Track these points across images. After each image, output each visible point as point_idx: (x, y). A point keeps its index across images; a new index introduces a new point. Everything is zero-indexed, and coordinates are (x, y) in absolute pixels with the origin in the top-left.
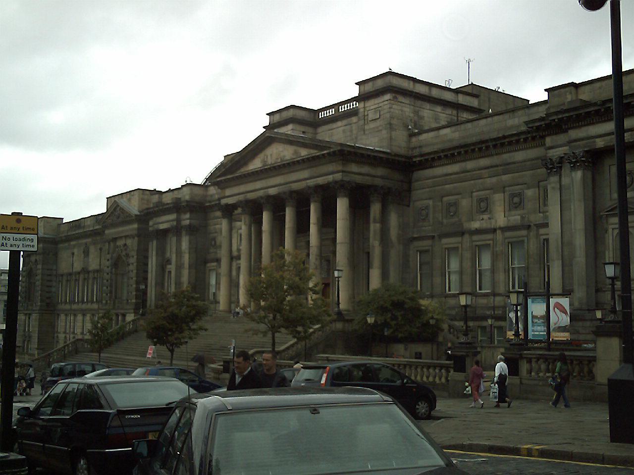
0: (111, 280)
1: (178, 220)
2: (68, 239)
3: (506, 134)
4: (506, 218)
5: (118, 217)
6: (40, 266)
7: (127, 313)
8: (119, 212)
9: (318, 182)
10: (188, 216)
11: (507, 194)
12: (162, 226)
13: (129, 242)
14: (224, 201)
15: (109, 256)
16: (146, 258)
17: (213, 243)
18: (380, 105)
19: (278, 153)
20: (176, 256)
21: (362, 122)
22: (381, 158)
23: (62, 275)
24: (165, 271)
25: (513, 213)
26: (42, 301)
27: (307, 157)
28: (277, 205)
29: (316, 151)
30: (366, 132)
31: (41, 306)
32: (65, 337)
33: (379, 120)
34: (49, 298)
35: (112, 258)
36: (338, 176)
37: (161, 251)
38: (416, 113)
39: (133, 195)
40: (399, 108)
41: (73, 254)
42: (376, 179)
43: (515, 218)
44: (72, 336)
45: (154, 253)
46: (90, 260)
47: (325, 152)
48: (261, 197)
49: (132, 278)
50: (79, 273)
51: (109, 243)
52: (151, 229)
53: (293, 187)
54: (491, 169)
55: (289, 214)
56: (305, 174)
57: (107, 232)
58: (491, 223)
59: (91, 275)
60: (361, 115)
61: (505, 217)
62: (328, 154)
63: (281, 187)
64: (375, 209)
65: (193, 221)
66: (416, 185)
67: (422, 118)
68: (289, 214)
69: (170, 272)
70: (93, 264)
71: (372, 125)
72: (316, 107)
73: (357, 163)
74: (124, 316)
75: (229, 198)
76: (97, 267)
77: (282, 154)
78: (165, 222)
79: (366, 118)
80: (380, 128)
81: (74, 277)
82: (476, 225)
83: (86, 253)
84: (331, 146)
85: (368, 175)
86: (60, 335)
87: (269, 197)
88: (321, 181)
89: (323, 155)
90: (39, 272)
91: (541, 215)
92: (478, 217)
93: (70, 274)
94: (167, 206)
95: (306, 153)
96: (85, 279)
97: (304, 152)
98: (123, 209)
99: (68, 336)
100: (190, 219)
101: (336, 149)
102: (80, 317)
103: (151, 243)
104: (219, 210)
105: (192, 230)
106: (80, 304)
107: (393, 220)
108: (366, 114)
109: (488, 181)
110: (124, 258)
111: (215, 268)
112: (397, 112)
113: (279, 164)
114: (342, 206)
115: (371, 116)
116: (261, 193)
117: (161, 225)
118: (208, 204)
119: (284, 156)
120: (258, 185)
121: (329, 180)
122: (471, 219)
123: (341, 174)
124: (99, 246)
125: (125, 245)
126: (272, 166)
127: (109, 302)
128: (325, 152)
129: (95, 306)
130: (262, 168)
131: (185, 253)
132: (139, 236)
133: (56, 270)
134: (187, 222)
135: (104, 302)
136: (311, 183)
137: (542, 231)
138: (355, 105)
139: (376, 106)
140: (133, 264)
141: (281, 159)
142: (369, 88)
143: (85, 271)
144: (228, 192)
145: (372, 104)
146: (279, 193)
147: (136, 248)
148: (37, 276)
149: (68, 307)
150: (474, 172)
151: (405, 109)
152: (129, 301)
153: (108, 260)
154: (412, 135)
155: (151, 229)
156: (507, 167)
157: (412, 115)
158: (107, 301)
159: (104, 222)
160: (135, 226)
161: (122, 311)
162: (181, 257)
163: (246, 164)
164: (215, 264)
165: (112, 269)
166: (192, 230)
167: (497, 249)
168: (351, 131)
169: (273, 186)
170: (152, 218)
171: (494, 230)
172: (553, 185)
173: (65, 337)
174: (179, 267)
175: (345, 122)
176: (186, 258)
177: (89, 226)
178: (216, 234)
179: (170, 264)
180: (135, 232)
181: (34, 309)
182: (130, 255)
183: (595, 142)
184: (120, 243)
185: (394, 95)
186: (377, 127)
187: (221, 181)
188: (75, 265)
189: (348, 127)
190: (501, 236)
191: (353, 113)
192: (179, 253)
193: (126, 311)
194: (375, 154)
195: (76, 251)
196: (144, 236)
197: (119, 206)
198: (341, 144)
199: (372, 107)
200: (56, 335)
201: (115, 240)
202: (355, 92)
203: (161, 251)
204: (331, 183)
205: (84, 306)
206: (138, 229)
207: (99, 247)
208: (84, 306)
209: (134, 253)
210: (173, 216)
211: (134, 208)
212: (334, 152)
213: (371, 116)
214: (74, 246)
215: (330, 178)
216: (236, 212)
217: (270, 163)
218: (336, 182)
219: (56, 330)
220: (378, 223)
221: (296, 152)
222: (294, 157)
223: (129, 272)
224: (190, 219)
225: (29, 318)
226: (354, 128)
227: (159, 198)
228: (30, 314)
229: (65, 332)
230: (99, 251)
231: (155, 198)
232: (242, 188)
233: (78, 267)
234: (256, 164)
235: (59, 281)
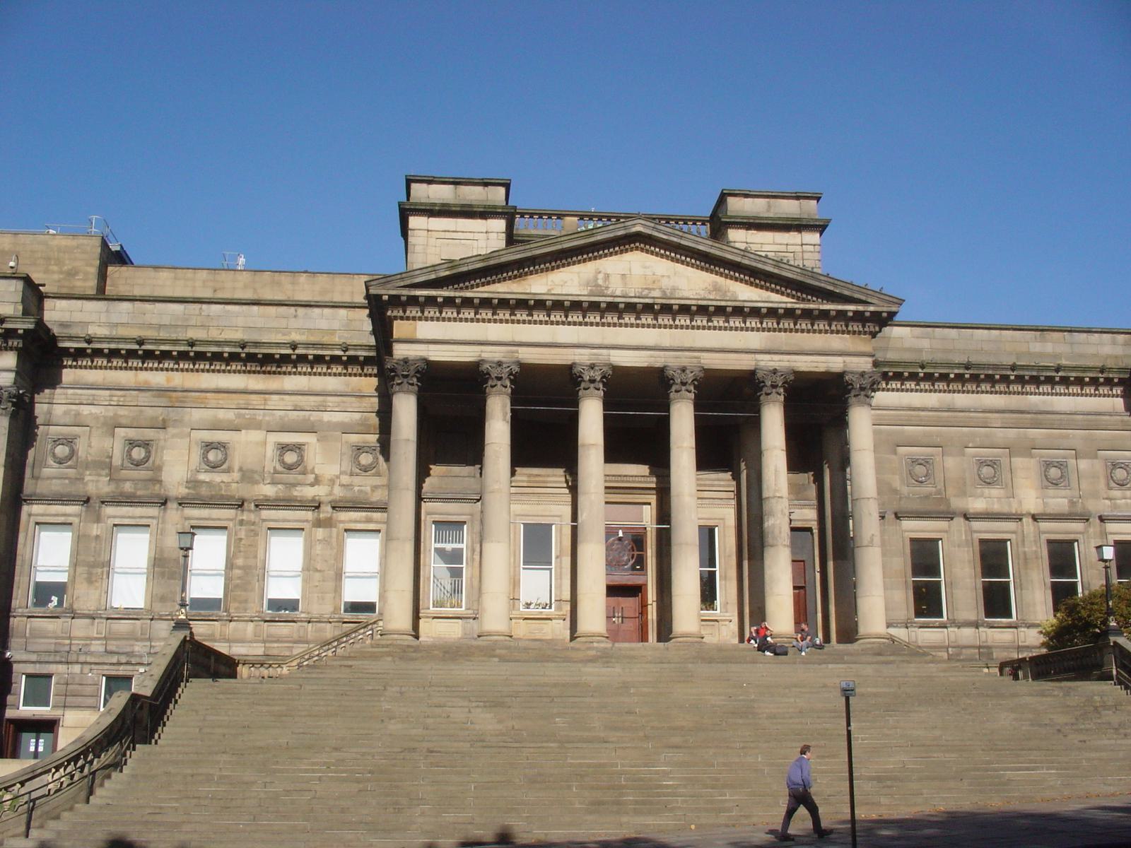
3: (1018, 363)
9: (793, 364)
18: (791, 248)
25: (1051, 492)
43: (1058, 501)
54: (1007, 415)
56: (754, 339)
58: (1010, 505)
63: (662, 353)
75: (432, 347)
77: (665, 283)
82: (977, 505)
84: (869, 300)
91: (1107, 502)
92: (979, 491)
101: (885, 309)
109: (1000, 433)
119: (674, 289)
121: (830, 365)
122: (963, 493)
139: (783, 248)
150: (972, 414)
156: (1039, 418)
167: (1026, 549)
171: (1018, 518)
190: (1032, 528)
215: (835, 364)
221: (716, 288)
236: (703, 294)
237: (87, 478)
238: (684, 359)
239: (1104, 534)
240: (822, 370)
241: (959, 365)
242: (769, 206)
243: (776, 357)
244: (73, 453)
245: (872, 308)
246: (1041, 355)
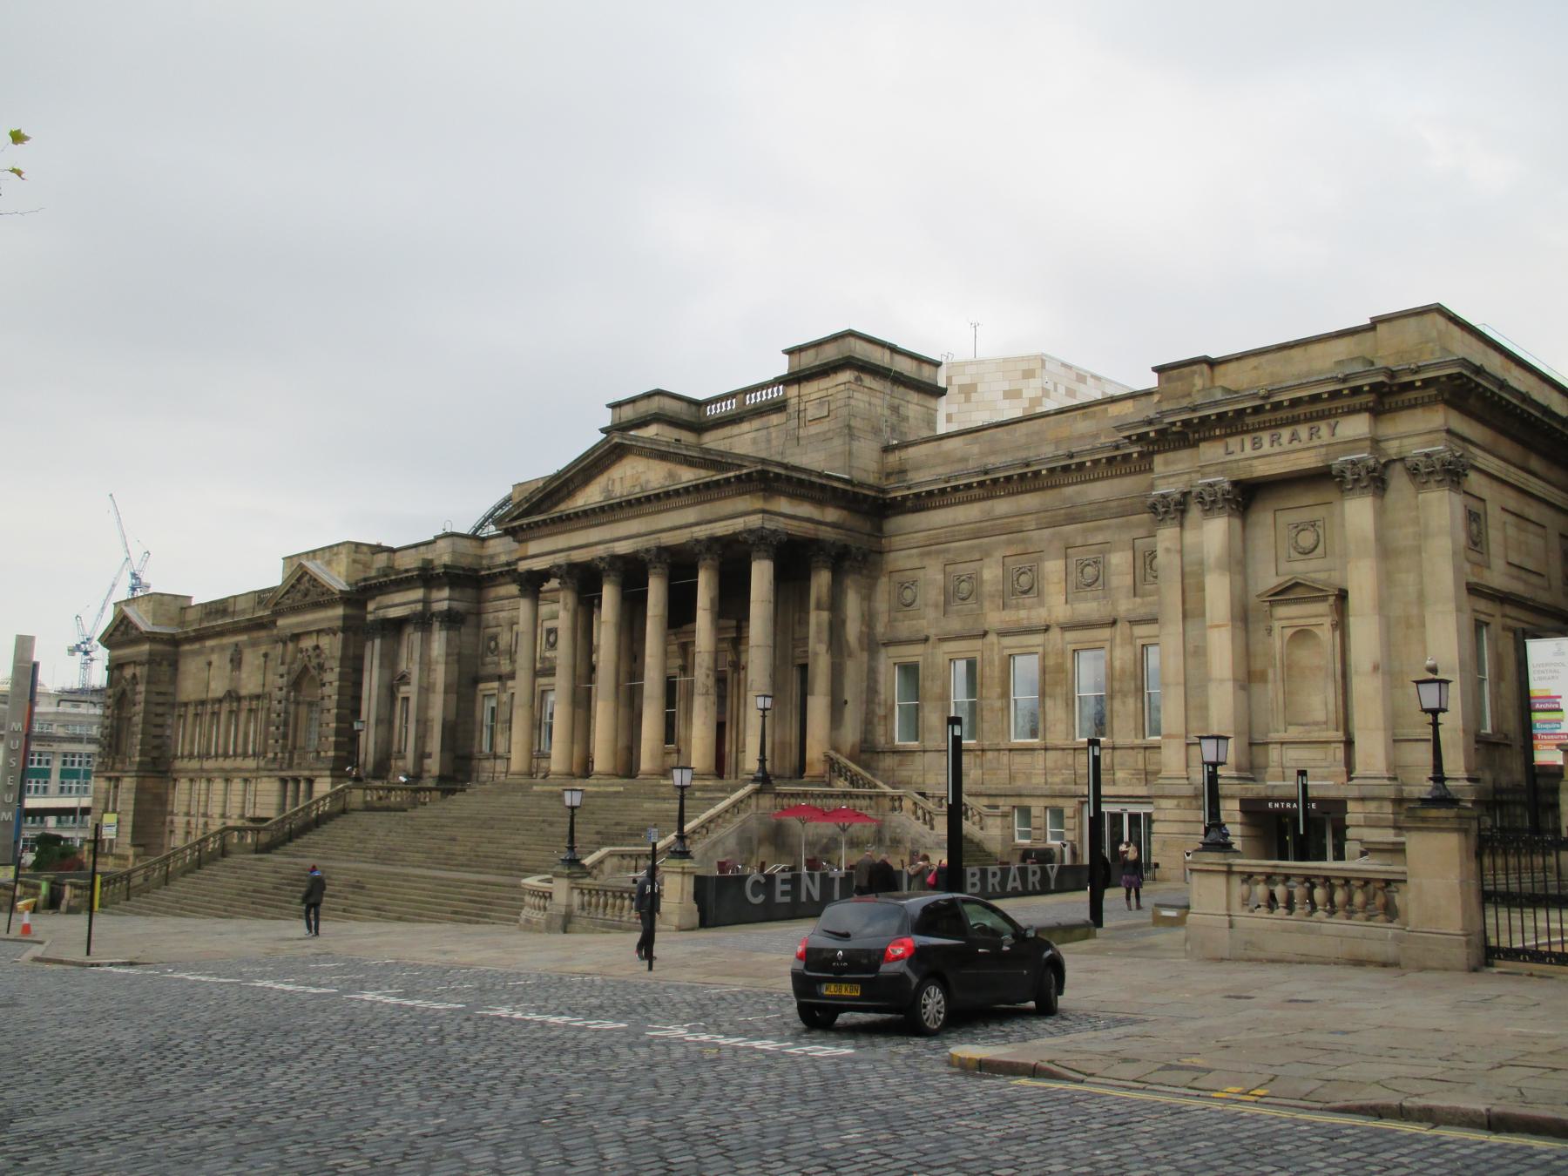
0: (286, 712)
1: (426, 602)
2: (201, 636)
4: (1069, 606)
5: (306, 595)
6: (141, 688)
7: (317, 777)
8: (307, 585)
9: (713, 531)
10: (446, 593)
11: (1072, 562)
12: (393, 613)
13: (325, 642)
14: (523, 566)
15: (283, 669)
16: (359, 671)
17: (493, 644)
18: (830, 392)
19: (633, 476)
20: (420, 669)
21: (793, 423)
22: (835, 489)
23: (186, 705)
24: (397, 698)
26: (142, 753)
27: (694, 483)
28: (631, 572)
29: (711, 473)
30: (801, 442)
31: (141, 763)
32: (188, 823)
33: (828, 419)
34: (157, 747)
35: (289, 673)
36: (755, 521)
37: (390, 660)
38: (895, 409)
39: (336, 554)
40: (866, 398)
41: (210, 664)
42: (823, 528)
44: (202, 820)
45: (376, 662)
46: (244, 675)
47: (731, 474)
48: (602, 559)
49: (329, 710)
50: (220, 701)
51: (285, 643)
52: (370, 617)
53: (662, 541)
55: (656, 591)
56: (690, 515)
57: (280, 622)
59: (245, 705)
60: (791, 410)
61: (1066, 602)
62: (738, 478)
63: (640, 539)
64: (821, 582)
65: (455, 604)
66: (897, 541)
67: (906, 419)
68: (656, 591)
69: (406, 699)
70: (250, 682)
71: (814, 429)
72: (700, 396)
73: (792, 496)
74: (310, 781)
75: (535, 560)
76: (259, 690)
77: (643, 479)
78: (399, 604)
79: (802, 415)
80: (830, 435)
81: (209, 707)
83: (236, 662)
85: (809, 520)
86: (176, 819)
87: (615, 558)
88: (721, 529)
89: (728, 480)
90: (141, 698)
92: (1014, 602)
93: (203, 703)
94: (406, 575)
95: (692, 477)
96: (231, 712)
97: (687, 475)
98: (315, 580)
99: (193, 820)
100: (449, 599)
101: (753, 469)
102: (218, 785)
103: (369, 644)
104: (514, 581)
105: (452, 620)
106: (221, 759)
107: (852, 605)
108: (802, 408)
110: (314, 672)
111: (496, 692)
112: (862, 405)
113: (638, 496)
114: (761, 574)
115: (812, 412)
116: (600, 551)
117: (392, 609)
118: (483, 573)
119: (648, 482)
120: (594, 535)
121: (737, 527)
123: (760, 516)
124: (263, 649)
125: (317, 647)
126: (623, 499)
127: (280, 755)
128: (731, 474)
129: (251, 763)
130: (603, 504)
131: (437, 662)
132: (344, 630)
133: (173, 694)
134: (444, 606)
135: (271, 755)
136: (702, 532)
137: (1140, 630)
138: (777, 392)
139: (824, 393)
140: (331, 683)
141: (642, 487)
142: (809, 360)
143: (233, 696)
144: (533, 547)
145: (813, 389)
146: (637, 552)
147: (338, 654)
148: (135, 705)
149: (195, 764)
151: (874, 401)
152: (322, 754)
153: (282, 676)
154: (887, 449)
155: (370, 617)
157: (887, 412)
158: (276, 754)
159: (276, 604)
160: (339, 611)
161: (306, 773)
162: (429, 670)
163: (571, 494)
164: (496, 684)
165: (289, 692)
166: (452, 620)
168: (769, 441)
169: (624, 537)
170: (373, 598)
172: (1168, 544)
173: (188, 823)
174: (426, 690)
175: (756, 423)
176: (439, 675)
177: (243, 612)
178: (499, 629)
179: (408, 684)
180: (340, 623)
181: (126, 769)
182: (326, 666)
183: (1251, 466)
184: (307, 643)
185: (856, 373)
186: (825, 433)
187: (521, 526)
188: (213, 685)
189: (764, 432)
191: (779, 406)
192: (426, 664)
193: (315, 773)
194: (824, 482)
195: (214, 658)
196: (356, 630)
197: (307, 573)
198: (763, 461)
199: (814, 396)
200: (168, 818)
201: (296, 637)
202: (782, 367)
203: (390, 660)
204: (740, 533)
205: (228, 764)
206: (345, 618)
207: (262, 652)
208: (228, 764)
209: (335, 665)
210: (418, 594)
211: (337, 578)
212: (749, 475)
213: (812, 412)
214: (212, 649)
215: (738, 525)
216: (546, 586)
217: (618, 495)
218: (751, 531)
219: (169, 808)
220: (823, 609)
221: (671, 475)
222: (667, 484)
223: (323, 698)
224: (449, 599)
225: (116, 787)
226: (774, 435)
227: (389, 559)
228: (118, 779)
229: (188, 814)
230: (262, 659)
231: (381, 560)
232: (561, 541)
233: (218, 688)
234: (591, 495)
235: (180, 716)
236: (662, 481)
237: (502, 662)
238: (650, 542)
239: (1132, 638)
240: (731, 532)
241: (977, 474)
242: (817, 355)
243: (704, 527)
244: (497, 644)
245: (745, 471)
246: (1082, 437)
